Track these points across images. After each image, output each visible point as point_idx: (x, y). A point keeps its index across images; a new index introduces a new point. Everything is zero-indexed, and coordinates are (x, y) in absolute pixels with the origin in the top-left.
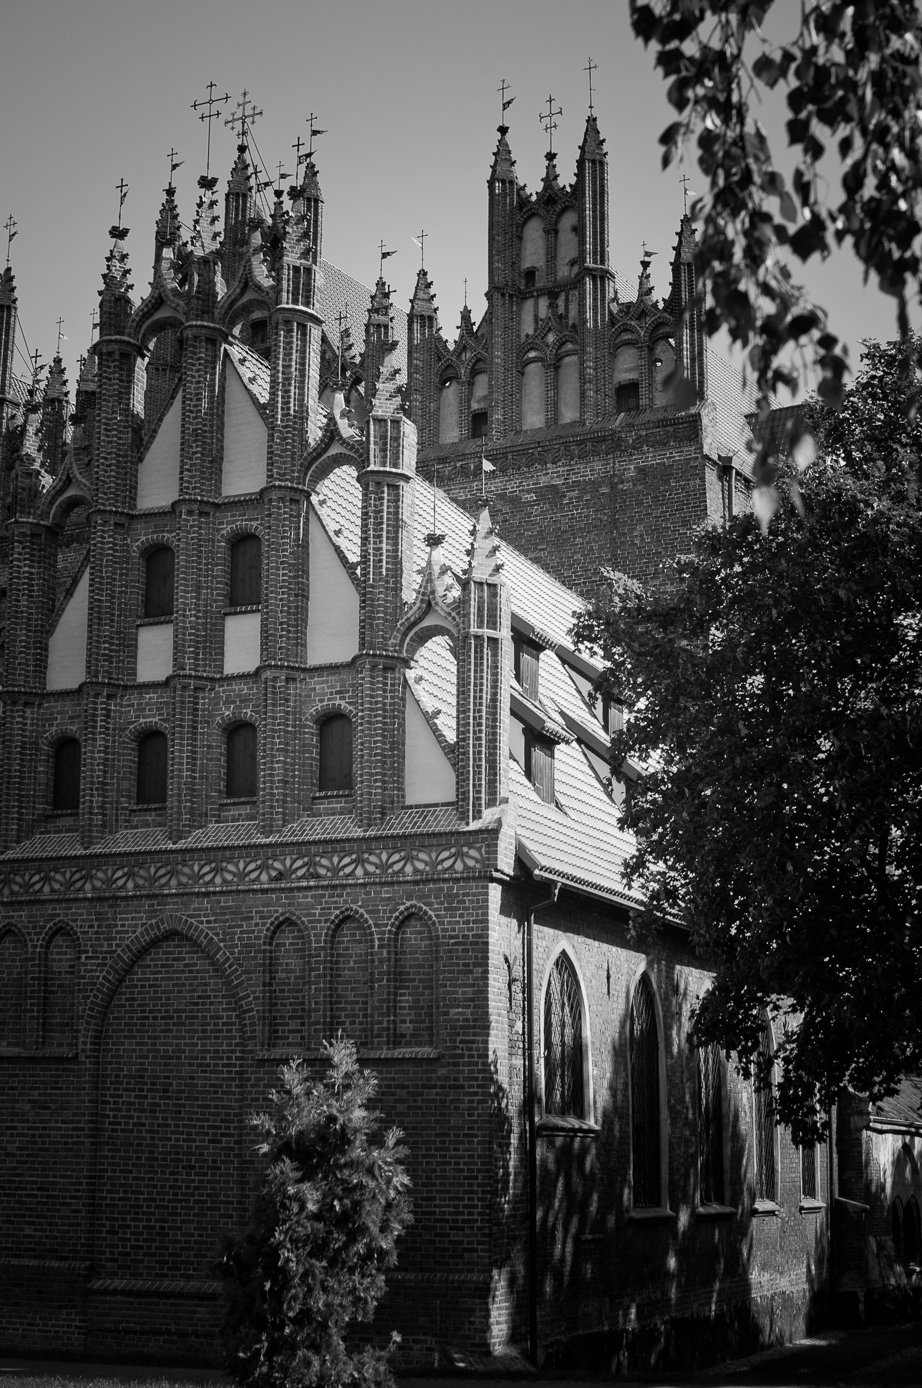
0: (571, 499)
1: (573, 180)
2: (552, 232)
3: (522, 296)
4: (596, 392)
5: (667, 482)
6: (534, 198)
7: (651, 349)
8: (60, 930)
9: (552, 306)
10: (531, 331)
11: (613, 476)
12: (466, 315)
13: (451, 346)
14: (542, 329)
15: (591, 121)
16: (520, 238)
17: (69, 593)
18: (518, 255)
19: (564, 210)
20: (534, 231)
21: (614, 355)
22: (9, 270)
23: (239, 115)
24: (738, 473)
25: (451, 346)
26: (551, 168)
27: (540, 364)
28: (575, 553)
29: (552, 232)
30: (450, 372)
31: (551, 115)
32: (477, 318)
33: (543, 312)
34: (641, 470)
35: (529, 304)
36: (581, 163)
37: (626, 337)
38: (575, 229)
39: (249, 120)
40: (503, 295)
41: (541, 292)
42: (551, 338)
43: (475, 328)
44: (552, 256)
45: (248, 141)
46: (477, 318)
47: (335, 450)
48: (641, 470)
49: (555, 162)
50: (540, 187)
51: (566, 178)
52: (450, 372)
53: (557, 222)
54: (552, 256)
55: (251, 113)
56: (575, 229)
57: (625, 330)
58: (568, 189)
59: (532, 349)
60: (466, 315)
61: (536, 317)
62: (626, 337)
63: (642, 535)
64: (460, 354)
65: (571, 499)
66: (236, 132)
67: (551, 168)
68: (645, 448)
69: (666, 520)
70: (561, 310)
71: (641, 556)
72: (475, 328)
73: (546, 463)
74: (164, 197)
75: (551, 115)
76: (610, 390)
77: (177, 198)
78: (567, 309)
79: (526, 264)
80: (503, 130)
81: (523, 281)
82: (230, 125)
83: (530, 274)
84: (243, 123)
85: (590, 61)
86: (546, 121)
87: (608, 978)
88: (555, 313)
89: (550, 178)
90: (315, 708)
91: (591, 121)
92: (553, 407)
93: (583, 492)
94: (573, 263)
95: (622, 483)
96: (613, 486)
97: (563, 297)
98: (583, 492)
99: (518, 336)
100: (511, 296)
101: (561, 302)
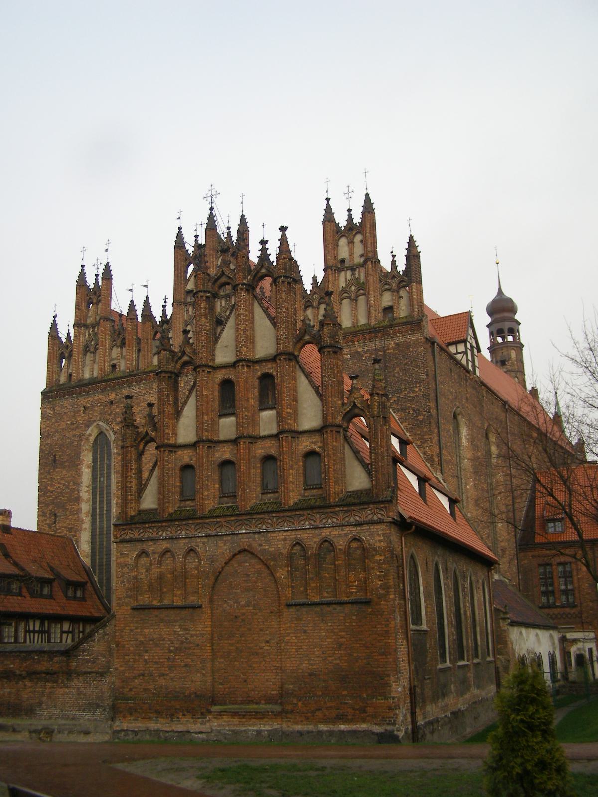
0: (366, 357)
1: (360, 220)
2: (351, 242)
3: (339, 271)
4: (375, 311)
5: (408, 349)
6: (343, 228)
7: (398, 292)
8: (192, 550)
9: (353, 274)
10: (344, 286)
11: (384, 347)
12: (315, 279)
13: (309, 292)
14: (349, 284)
15: (367, 195)
16: (338, 245)
17: (185, 403)
18: (337, 253)
19: (356, 233)
20: (343, 241)
21: (381, 295)
22: (108, 263)
24: (437, 345)
25: (309, 292)
26: (350, 216)
27: (348, 300)
28: (369, 380)
29: (351, 242)
30: (309, 304)
31: (349, 193)
32: (320, 280)
33: (349, 277)
34: (397, 344)
35: (343, 274)
36: (363, 214)
37: (387, 287)
38: (362, 241)
39: (214, 197)
40: (332, 270)
42: (353, 288)
43: (319, 284)
44: (351, 254)
45: (214, 206)
46: (320, 280)
47: (307, 337)
48: (397, 344)
49: (351, 213)
50: (345, 223)
51: (357, 219)
52: (309, 304)
53: (353, 238)
54: (351, 254)
56: (362, 241)
57: (386, 284)
58: (358, 224)
59: (345, 293)
60: (315, 279)
61: (346, 279)
62: (387, 287)
63: (398, 372)
64: (313, 296)
65: (366, 357)
67: (350, 216)
68: (398, 335)
69: (409, 365)
70: (357, 276)
71: (398, 381)
72: (319, 284)
73: (354, 342)
74: (178, 230)
75: (349, 193)
76: (381, 310)
77: (183, 231)
78: (359, 275)
79: (340, 257)
81: (339, 264)
82: (206, 199)
83: (343, 261)
84: (212, 197)
85: (365, 169)
86: (347, 195)
87: (427, 563)
88: (354, 277)
89: (350, 218)
91: (367, 195)
92: (355, 317)
93: (372, 354)
94: (362, 256)
95: (388, 349)
96: (384, 351)
97: (357, 270)
98: (372, 354)
99: (339, 287)
100: (335, 270)
101: (357, 273)
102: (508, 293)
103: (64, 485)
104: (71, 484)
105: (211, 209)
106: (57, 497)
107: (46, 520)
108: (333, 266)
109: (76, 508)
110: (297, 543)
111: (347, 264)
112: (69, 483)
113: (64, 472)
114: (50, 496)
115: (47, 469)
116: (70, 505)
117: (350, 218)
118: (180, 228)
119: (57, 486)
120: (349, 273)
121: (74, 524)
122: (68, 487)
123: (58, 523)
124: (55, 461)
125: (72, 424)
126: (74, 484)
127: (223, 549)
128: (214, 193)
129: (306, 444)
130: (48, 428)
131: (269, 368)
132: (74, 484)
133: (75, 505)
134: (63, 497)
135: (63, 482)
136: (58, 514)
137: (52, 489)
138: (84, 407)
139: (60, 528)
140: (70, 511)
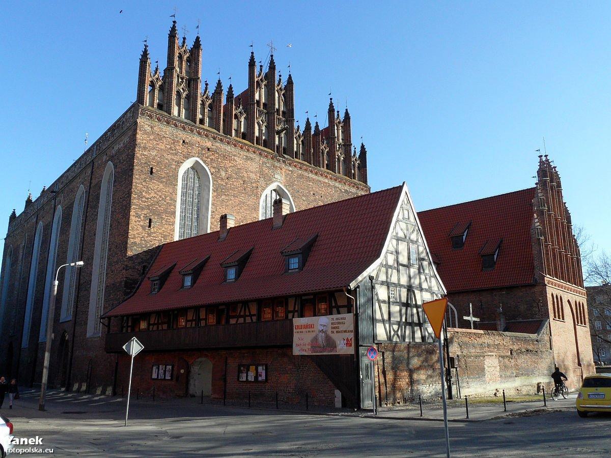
80: (331, 99)
103: (160, 197)
104: (168, 198)
105: (272, 56)
106: (152, 205)
107: (139, 221)
109: (172, 220)
112: (166, 197)
113: (161, 186)
114: (145, 202)
115: (143, 177)
116: (166, 216)
118: (252, 53)
119: (153, 195)
121: (169, 233)
122: (164, 200)
123: (153, 228)
124: (152, 173)
125: (171, 148)
126: (171, 199)
130: (144, 141)
132: (171, 199)
133: (171, 217)
134: (160, 206)
135: (160, 194)
136: (153, 220)
137: (147, 196)
138: (184, 142)
139: (154, 233)
140: (166, 221)
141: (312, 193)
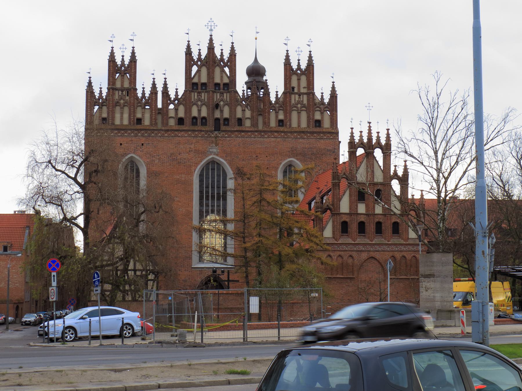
2: (299, 80)
8: (351, 256)
23: (210, 24)
26: (299, 63)
29: (299, 80)
33: (297, 99)
35: (293, 96)
39: (213, 27)
41: (296, 93)
50: (296, 67)
55: (214, 25)
61: (295, 100)
66: (209, 29)
67: (299, 63)
78: (303, 99)
89: (299, 65)
90: (393, 221)
97: (302, 96)
102: (262, 62)
105: (211, 36)
108: (289, 90)
110: (393, 256)
111: (296, 90)
117: (299, 65)
120: (297, 96)
127: (364, 256)
128: (213, 24)
129: (394, 219)
131: (379, 187)
141: (254, 156)
